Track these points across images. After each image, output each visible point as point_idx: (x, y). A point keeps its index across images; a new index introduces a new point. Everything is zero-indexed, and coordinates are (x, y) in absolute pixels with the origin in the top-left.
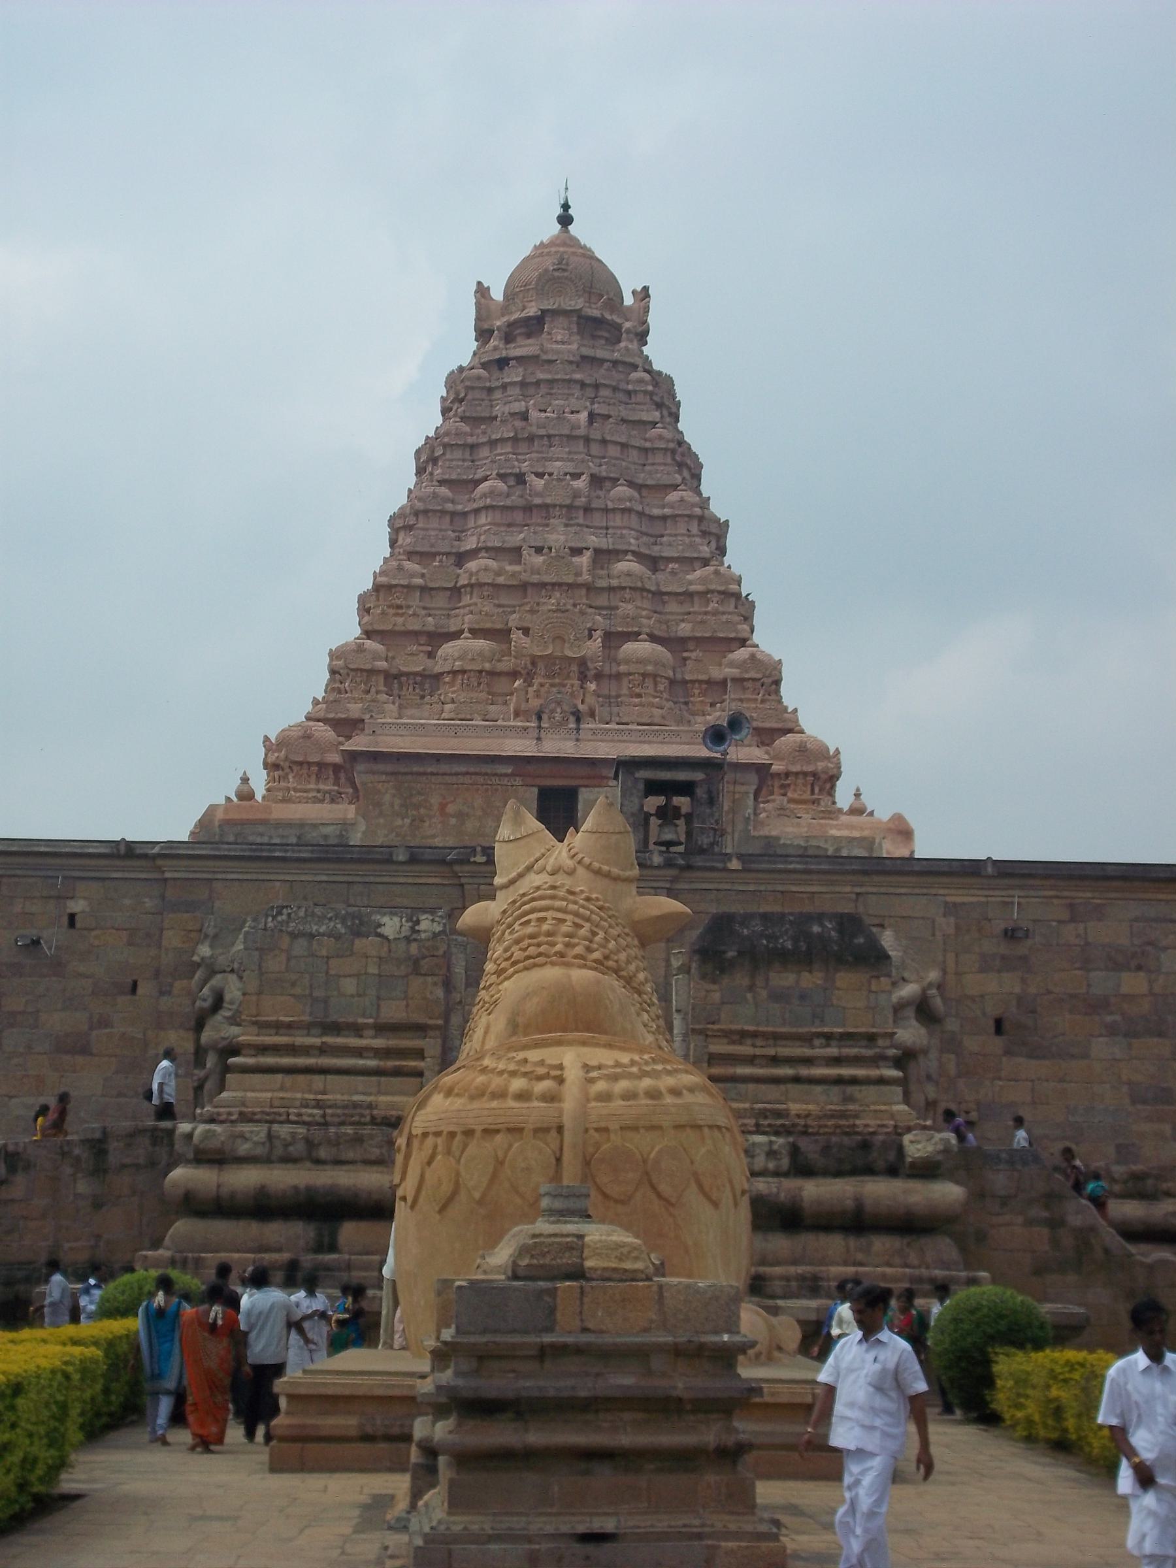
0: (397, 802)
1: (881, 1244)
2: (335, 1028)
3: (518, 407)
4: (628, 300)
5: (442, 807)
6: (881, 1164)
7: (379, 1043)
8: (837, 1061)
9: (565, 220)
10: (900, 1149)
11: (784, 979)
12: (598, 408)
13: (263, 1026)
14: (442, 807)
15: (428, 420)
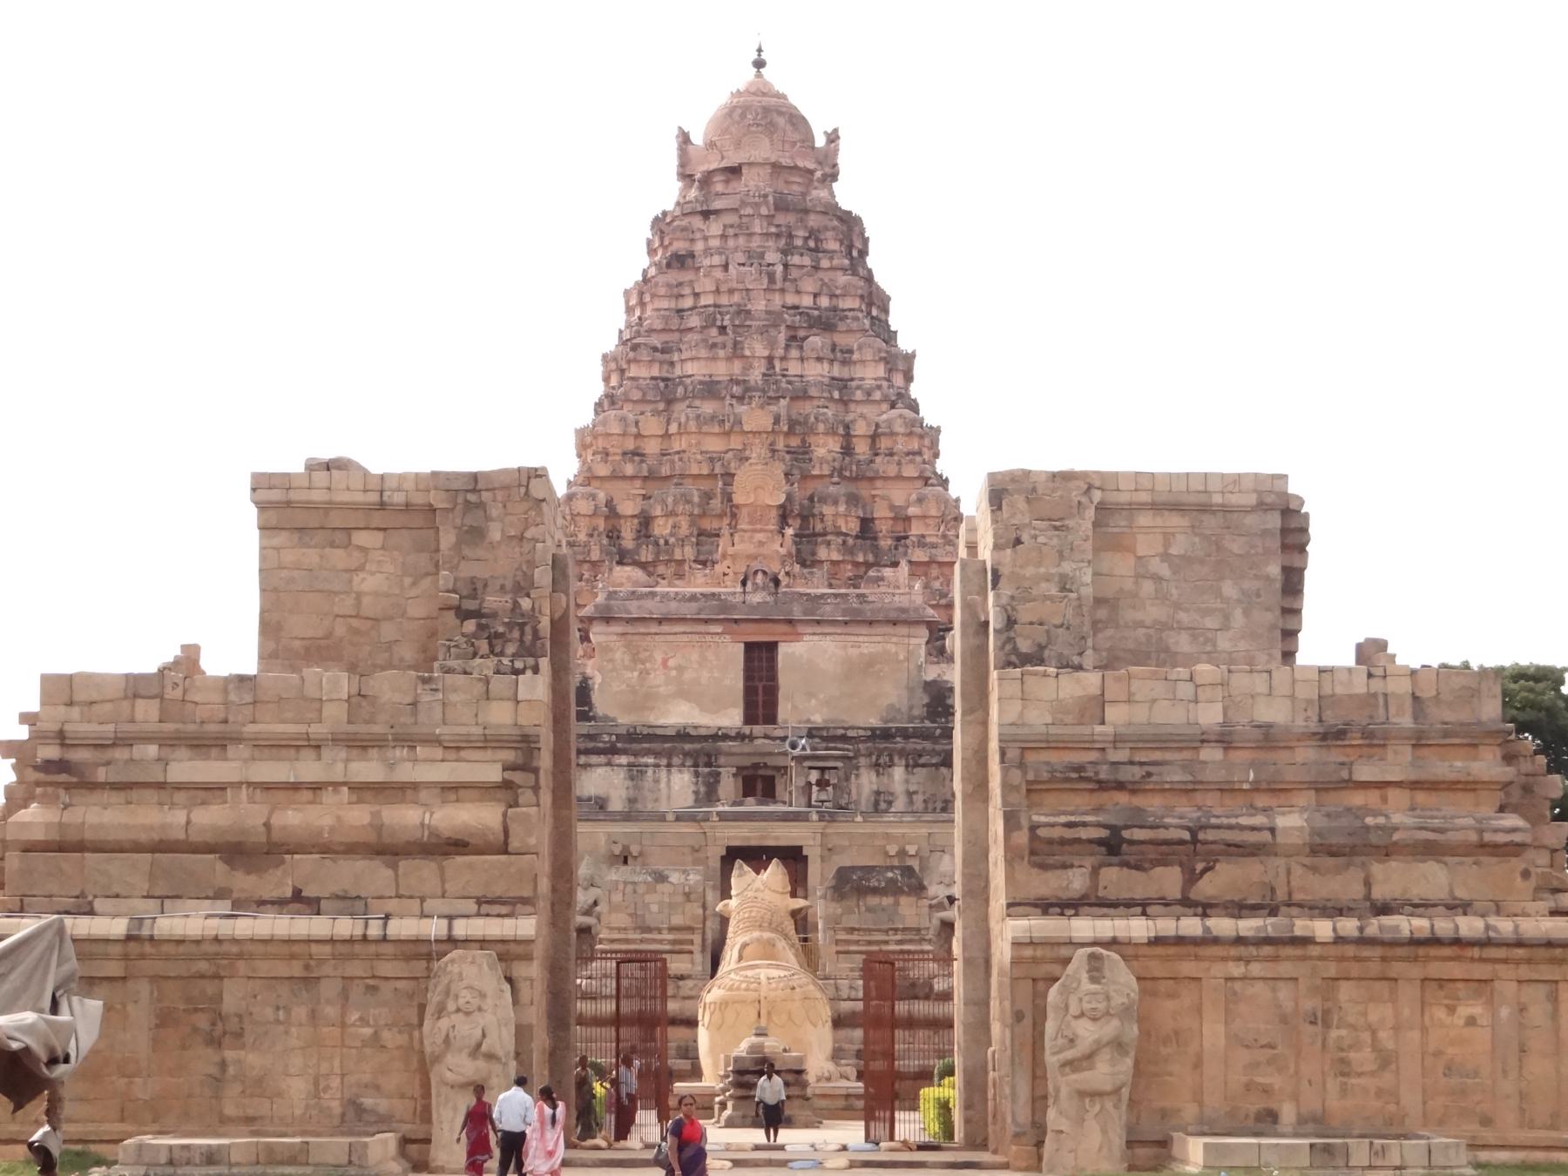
0: (627, 658)
1: (921, 1034)
2: (649, 930)
3: (717, 260)
4: (820, 141)
5: (665, 662)
6: (921, 994)
7: (671, 937)
8: (900, 942)
9: (759, 64)
10: (931, 987)
11: (873, 901)
12: (796, 260)
13: (611, 929)
14: (665, 662)
15: (634, 262)
